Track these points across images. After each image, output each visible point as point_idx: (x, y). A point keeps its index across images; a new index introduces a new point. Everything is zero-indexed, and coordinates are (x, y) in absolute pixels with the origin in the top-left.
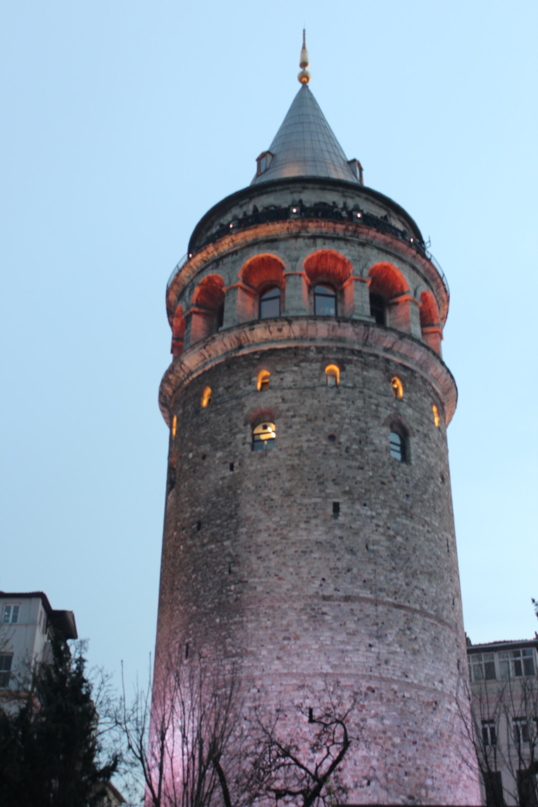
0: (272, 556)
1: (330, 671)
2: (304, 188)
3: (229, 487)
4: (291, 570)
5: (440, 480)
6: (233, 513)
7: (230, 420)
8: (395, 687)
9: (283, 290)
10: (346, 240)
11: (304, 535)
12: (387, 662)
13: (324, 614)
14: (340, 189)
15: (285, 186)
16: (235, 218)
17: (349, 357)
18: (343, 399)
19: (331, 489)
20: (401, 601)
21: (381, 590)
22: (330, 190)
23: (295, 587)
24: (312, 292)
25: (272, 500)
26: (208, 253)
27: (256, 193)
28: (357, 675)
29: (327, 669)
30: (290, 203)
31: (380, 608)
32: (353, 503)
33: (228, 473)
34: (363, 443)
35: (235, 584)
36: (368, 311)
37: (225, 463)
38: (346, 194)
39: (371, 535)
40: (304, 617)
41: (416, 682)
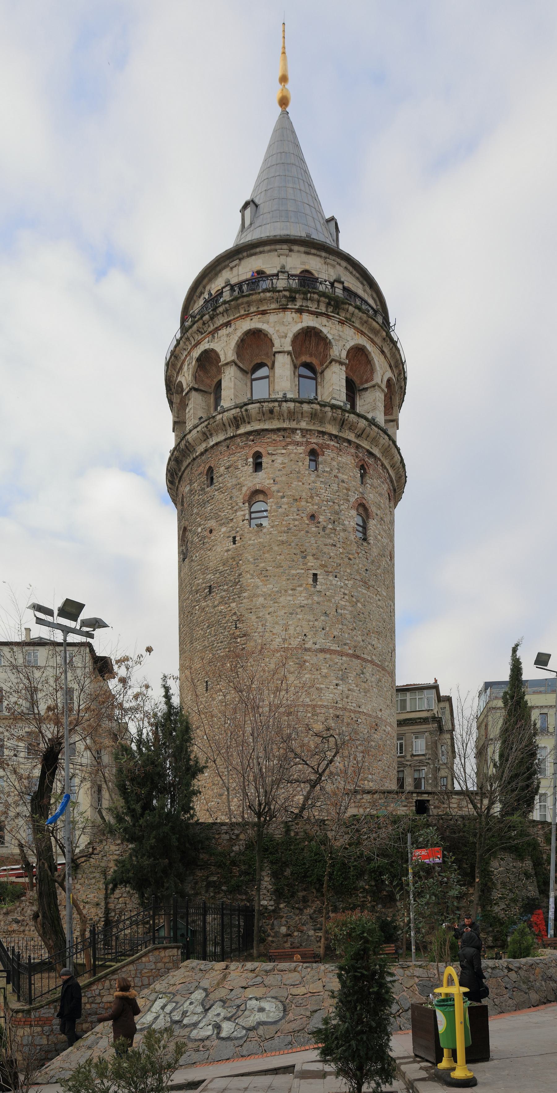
2: (291, 250)
3: (233, 558)
6: (237, 580)
7: (231, 498)
9: (272, 367)
10: (328, 316)
12: (347, 697)
14: (323, 254)
15: (273, 247)
16: (228, 284)
17: (327, 442)
21: (345, 644)
22: (314, 254)
24: (297, 374)
27: (245, 254)
30: (279, 269)
31: (344, 658)
32: (328, 575)
34: (336, 523)
35: (241, 637)
36: (344, 397)
38: (328, 261)
39: (340, 602)
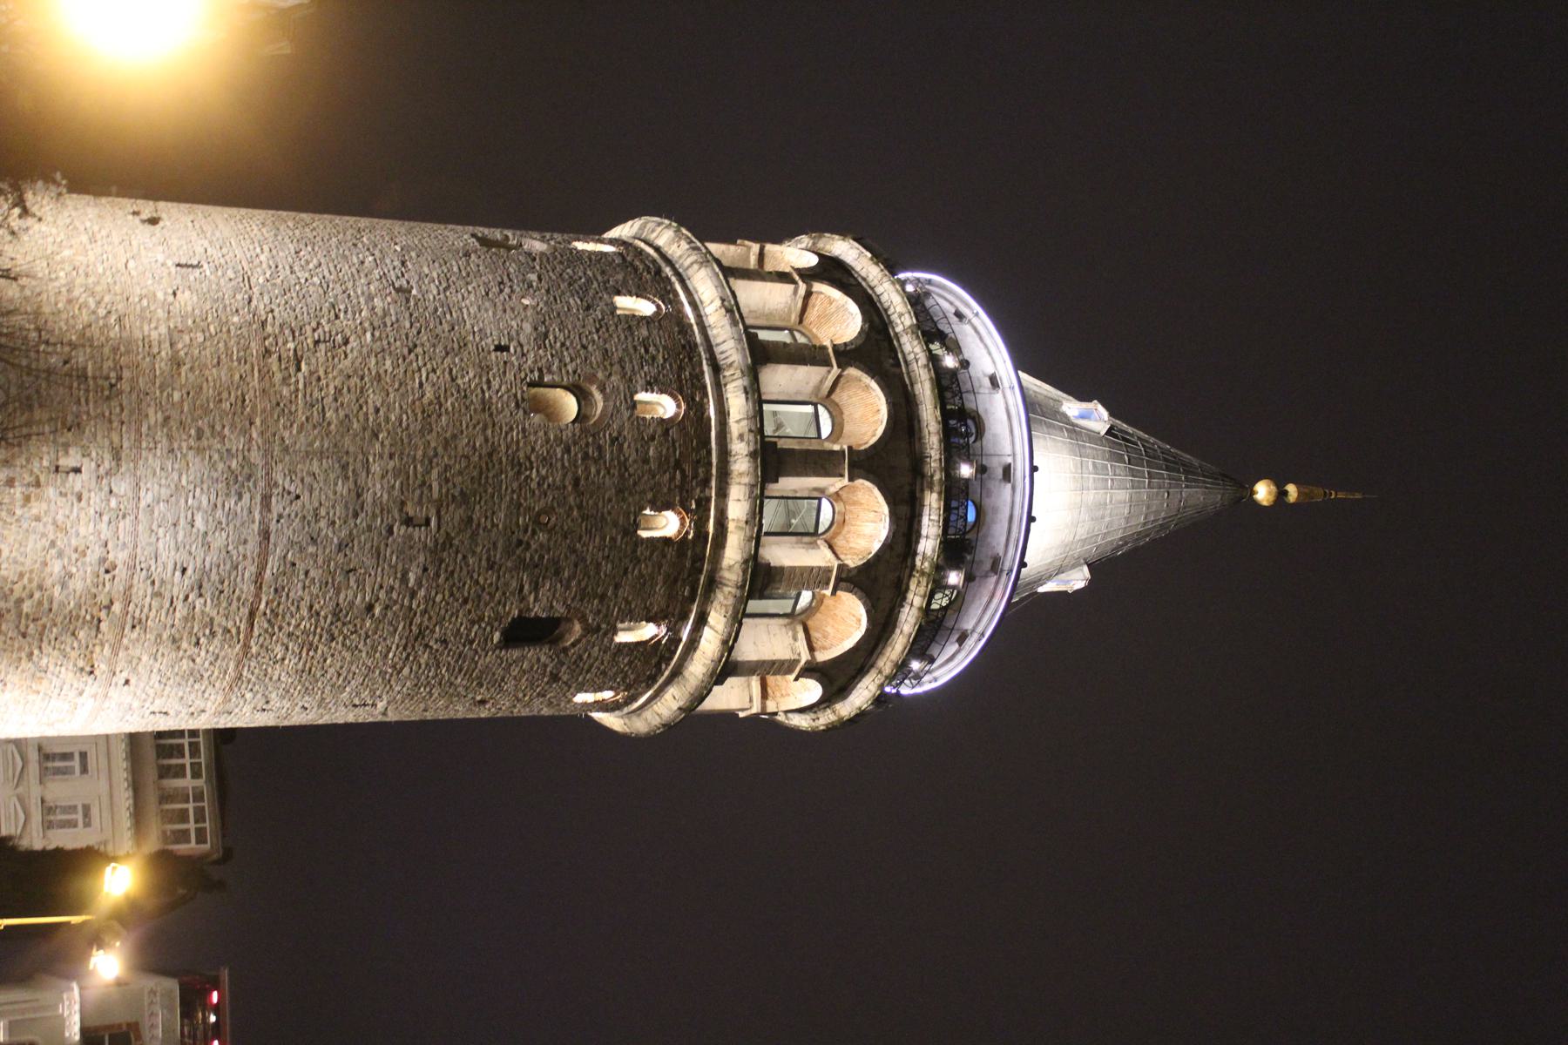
0: (342, 414)
1: (143, 504)
4: (317, 444)
5: (479, 698)
8: (117, 608)
11: (376, 468)
13: (240, 496)
18: (613, 539)
19: (454, 515)
20: (260, 624)
23: (286, 450)
25: (440, 416)
26: (901, 315)
28: (136, 546)
29: (146, 498)
31: (247, 589)
33: (490, 343)
37: (510, 340)
40: (234, 464)
41: (125, 641)
